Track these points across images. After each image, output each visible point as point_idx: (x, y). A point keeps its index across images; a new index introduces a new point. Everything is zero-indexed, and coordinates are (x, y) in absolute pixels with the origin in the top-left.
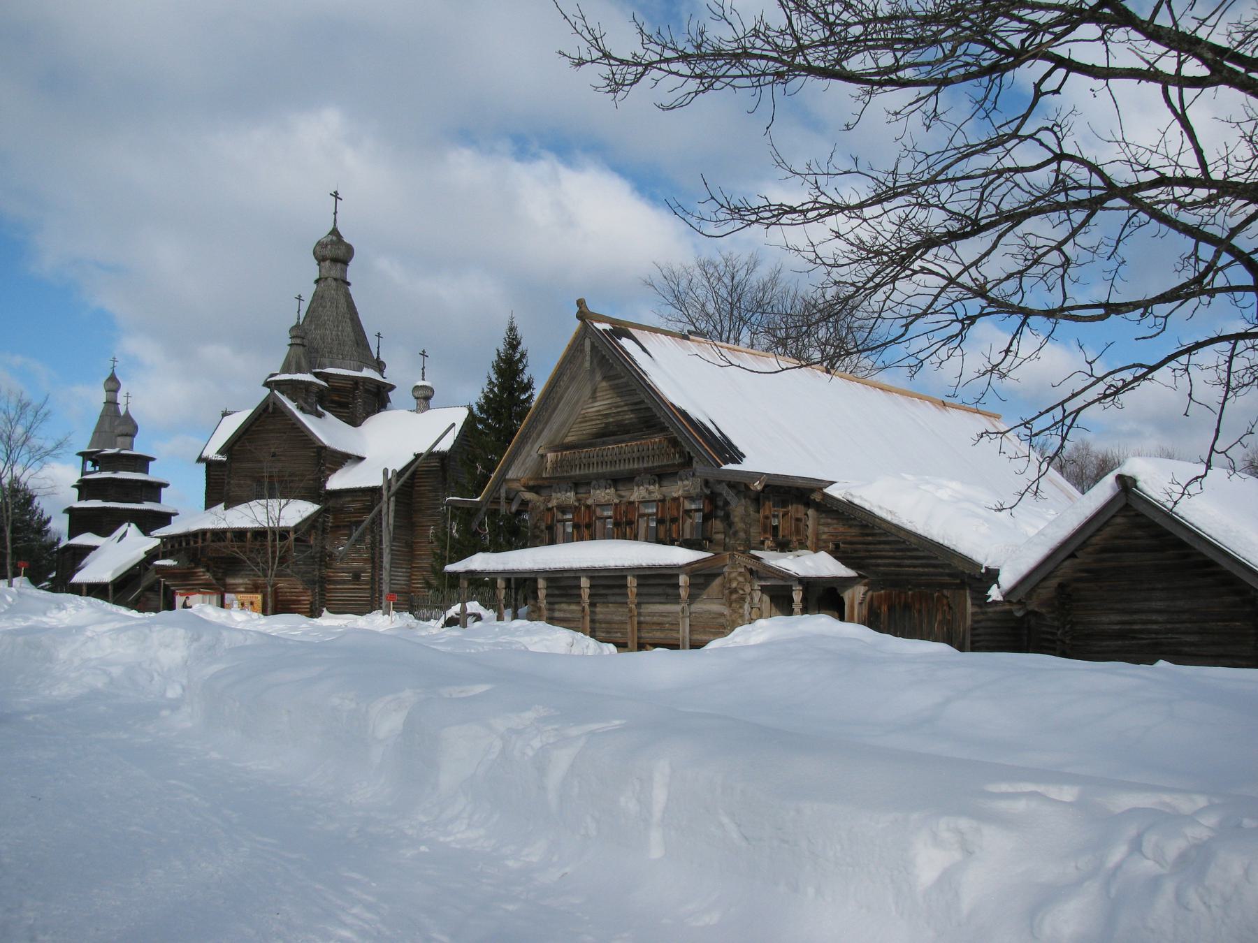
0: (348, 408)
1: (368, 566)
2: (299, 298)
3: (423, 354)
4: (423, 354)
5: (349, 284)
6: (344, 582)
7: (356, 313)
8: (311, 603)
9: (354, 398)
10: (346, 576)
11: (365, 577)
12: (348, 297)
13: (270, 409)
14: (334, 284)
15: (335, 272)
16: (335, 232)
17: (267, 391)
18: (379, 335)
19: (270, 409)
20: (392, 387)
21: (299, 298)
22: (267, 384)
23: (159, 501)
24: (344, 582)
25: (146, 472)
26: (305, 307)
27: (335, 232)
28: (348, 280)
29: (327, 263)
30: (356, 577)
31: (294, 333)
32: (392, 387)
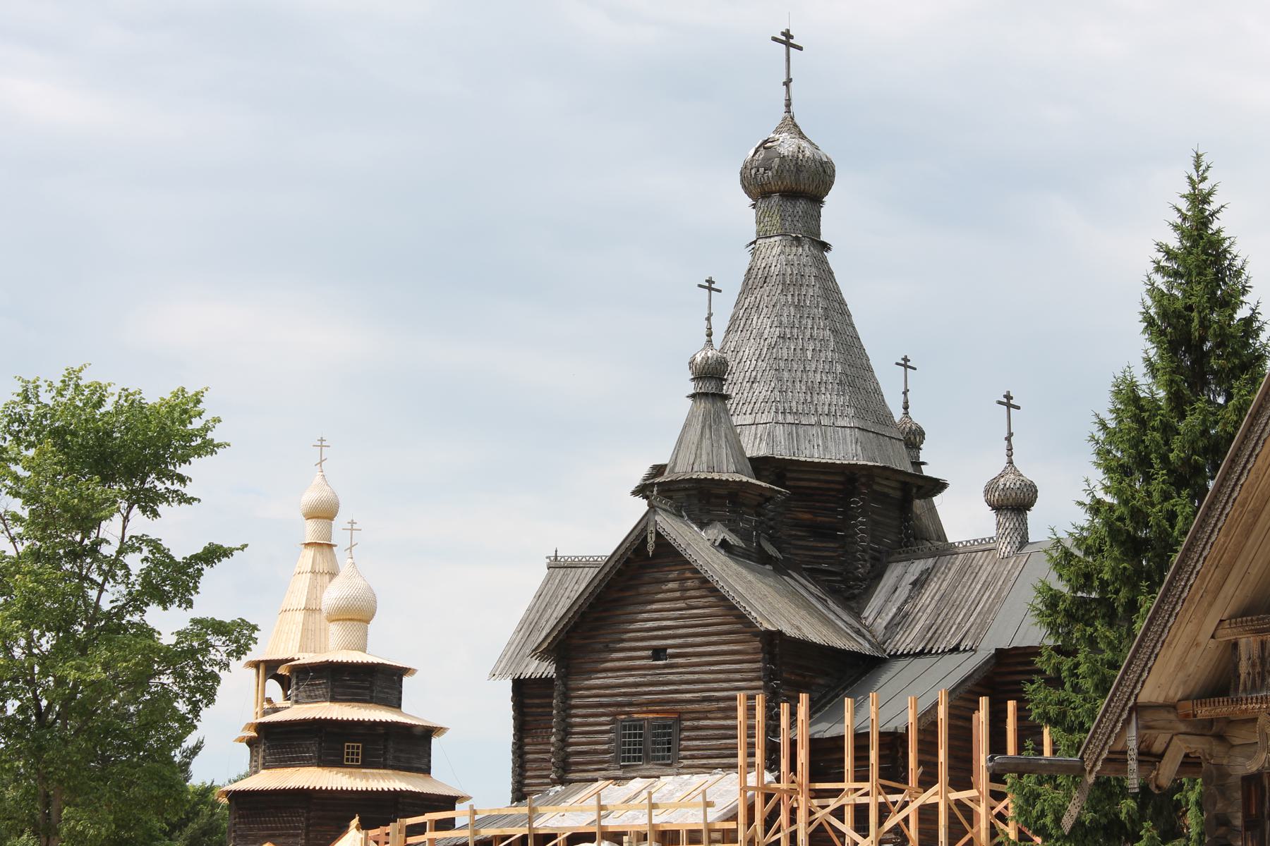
0: (835, 538)
2: (709, 286)
3: (1008, 402)
4: (1008, 402)
5: (825, 247)
7: (845, 313)
12: (826, 276)
13: (651, 548)
16: (791, 125)
17: (642, 505)
18: (905, 364)
19: (651, 548)
20: (938, 486)
21: (709, 286)
22: (642, 491)
23: (426, 770)
25: (396, 703)
26: (724, 307)
28: (824, 237)
29: (776, 198)
32: (938, 486)
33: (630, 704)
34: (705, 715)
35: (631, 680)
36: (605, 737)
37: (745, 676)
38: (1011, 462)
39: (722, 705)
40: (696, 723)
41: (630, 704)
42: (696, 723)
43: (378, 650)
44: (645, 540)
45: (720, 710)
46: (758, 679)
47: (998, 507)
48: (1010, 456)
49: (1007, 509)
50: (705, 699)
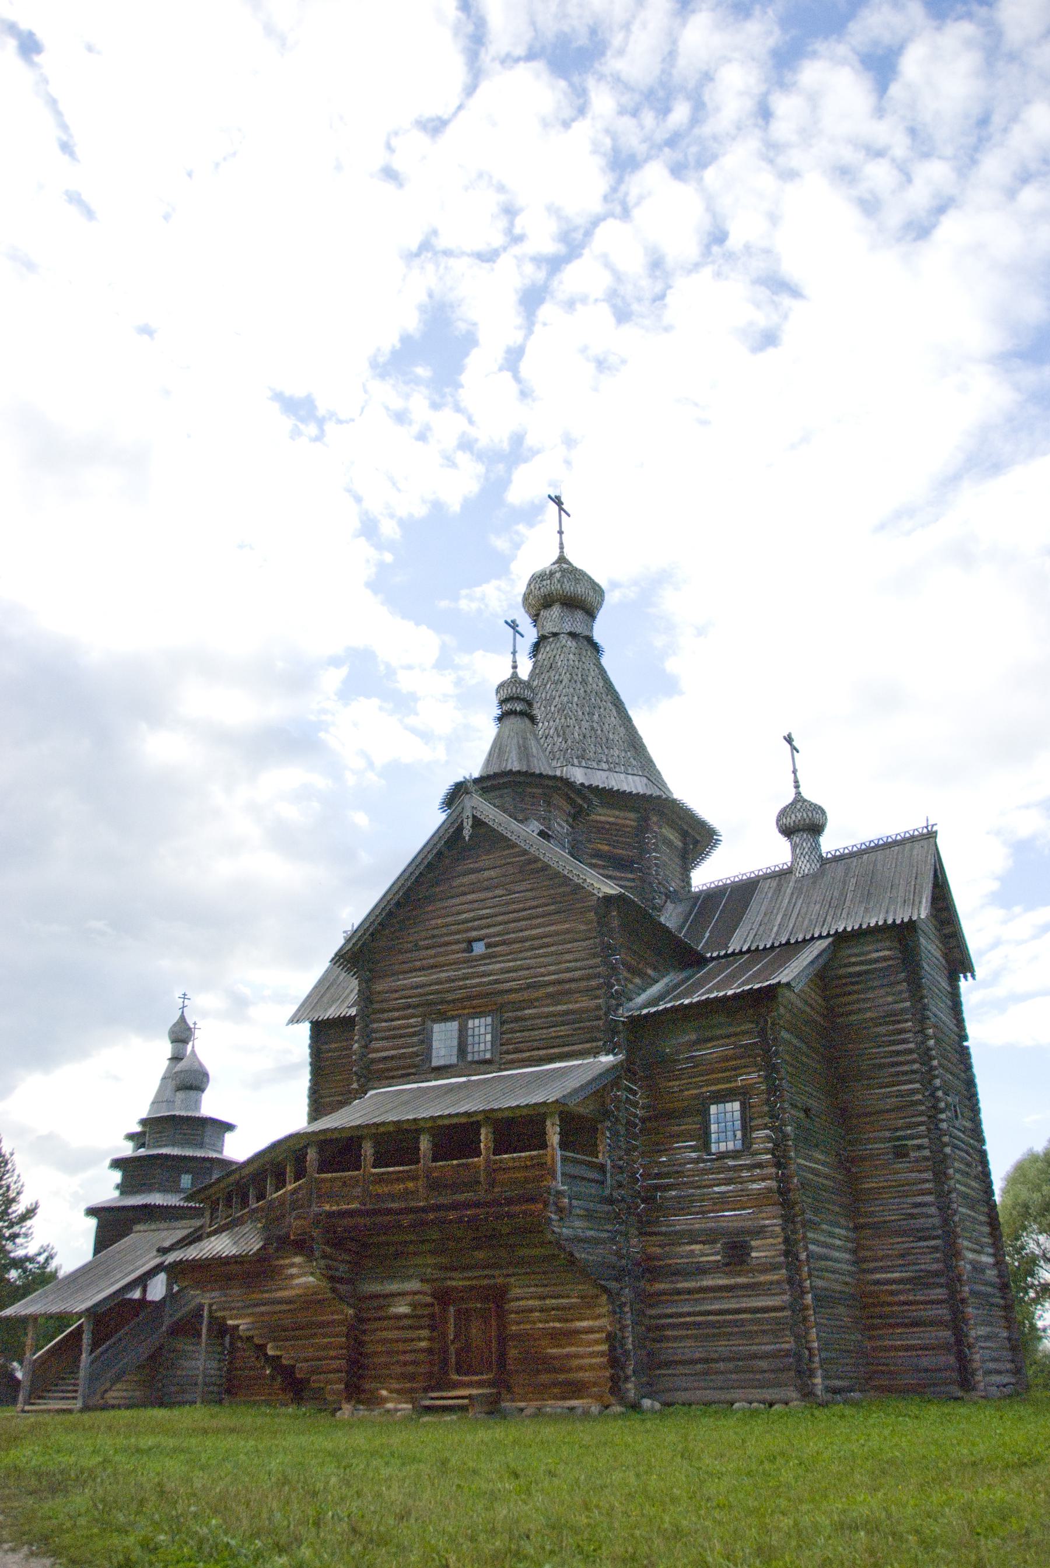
1: (771, 1220)
3: (789, 739)
5: (596, 648)
6: (702, 1271)
8: (610, 1338)
9: (643, 850)
10: (711, 1255)
11: (761, 1252)
13: (467, 833)
14: (571, 643)
15: (574, 622)
16: (562, 559)
24: (702, 1271)
25: (221, 1152)
27: (562, 559)
28: (598, 636)
30: (737, 1252)
31: (504, 694)
33: (442, 1002)
34: (531, 1003)
35: (443, 975)
36: (415, 1039)
37: (577, 955)
38: (798, 793)
39: (550, 989)
40: (519, 1014)
41: (442, 1002)
42: (519, 1014)
43: (210, 1106)
44: (460, 828)
45: (549, 995)
46: (595, 956)
47: (787, 831)
48: (797, 787)
49: (803, 830)
50: (529, 986)
